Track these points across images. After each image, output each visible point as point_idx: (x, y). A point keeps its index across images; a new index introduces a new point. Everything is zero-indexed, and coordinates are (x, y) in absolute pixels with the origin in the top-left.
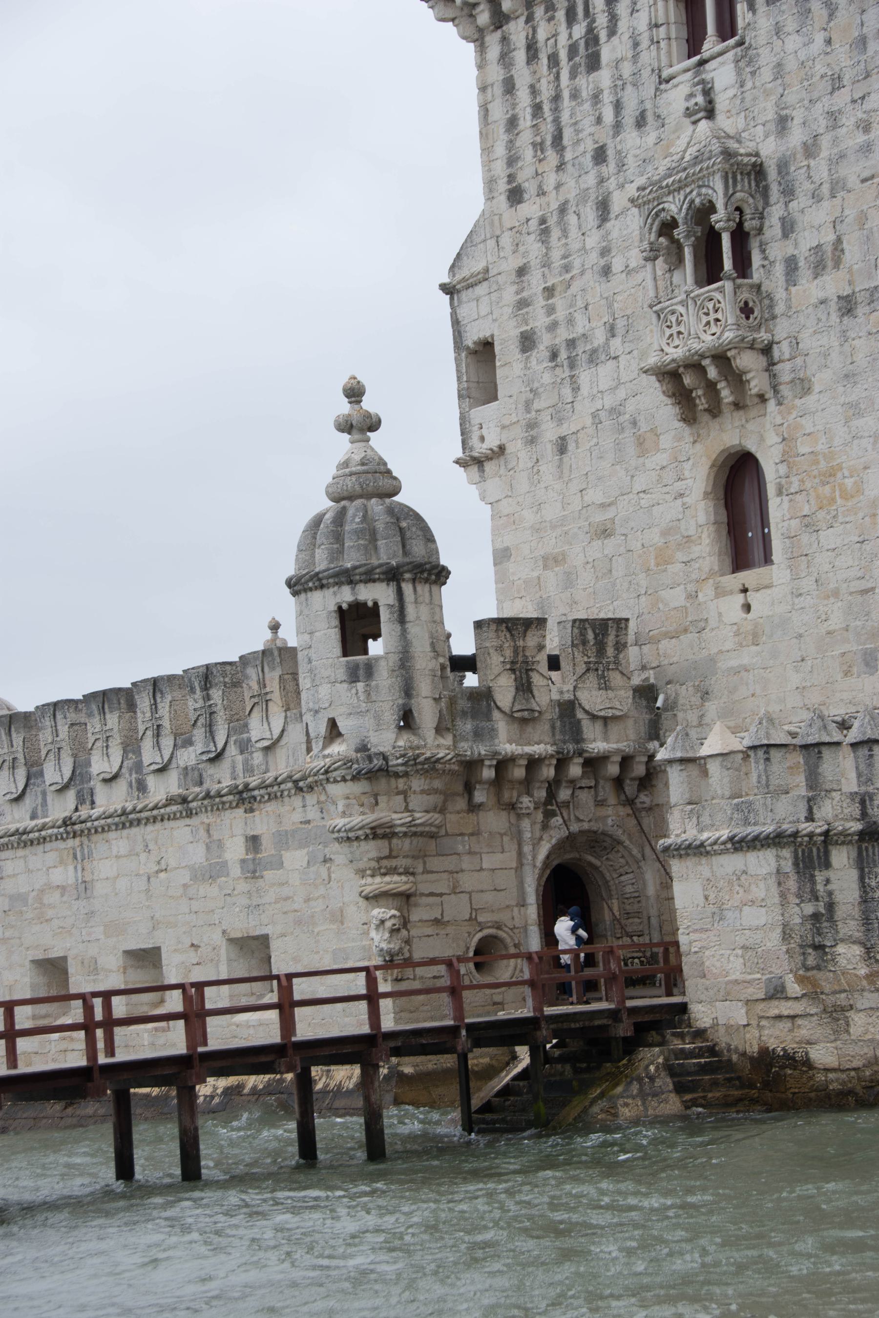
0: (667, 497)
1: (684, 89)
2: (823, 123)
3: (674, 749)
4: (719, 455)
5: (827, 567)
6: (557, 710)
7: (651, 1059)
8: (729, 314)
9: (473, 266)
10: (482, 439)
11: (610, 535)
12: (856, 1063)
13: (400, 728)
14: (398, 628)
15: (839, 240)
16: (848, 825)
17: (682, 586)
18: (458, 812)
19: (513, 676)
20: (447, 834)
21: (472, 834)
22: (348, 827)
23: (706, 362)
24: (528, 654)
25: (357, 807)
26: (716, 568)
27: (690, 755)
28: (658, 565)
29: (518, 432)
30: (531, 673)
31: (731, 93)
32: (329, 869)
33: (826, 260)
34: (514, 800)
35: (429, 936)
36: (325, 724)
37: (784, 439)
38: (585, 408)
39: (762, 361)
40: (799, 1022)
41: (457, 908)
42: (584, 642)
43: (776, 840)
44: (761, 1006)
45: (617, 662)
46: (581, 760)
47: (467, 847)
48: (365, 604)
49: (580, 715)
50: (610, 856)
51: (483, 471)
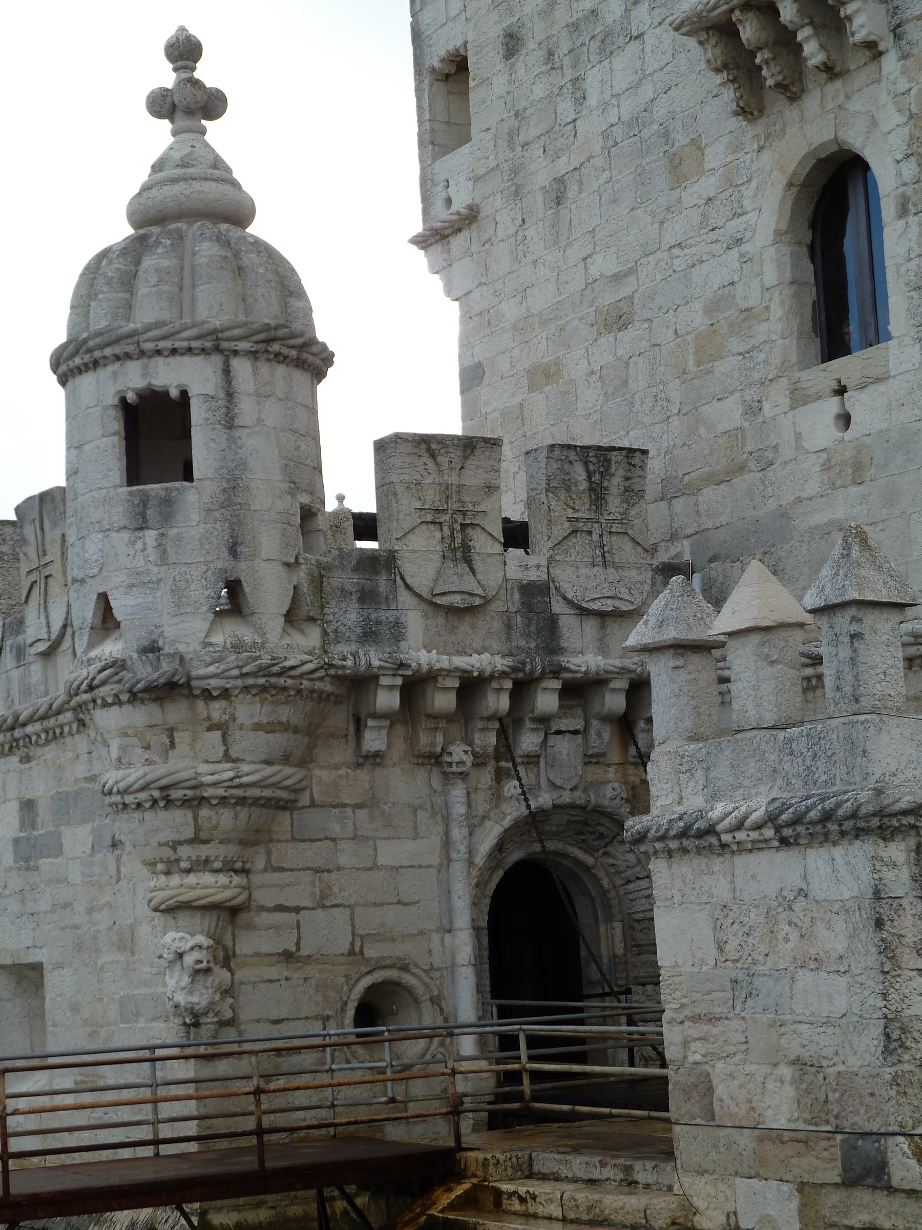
0: (716, 248)
3: (661, 625)
4: (800, 164)
6: (517, 596)
10: (449, 201)
11: (625, 326)
13: (219, 615)
17: (737, 395)
18: (336, 767)
19: (438, 535)
20: (313, 804)
22: (122, 786)
24: (465, 498)
25: (139, 751)
26: (794, 359)
27: (693, 636)
28: (699, 363)
30: (470, 532)
32: (118, 859)
34: (439, 749)
35: (271, 981)
36: (92, 605)
37: (911, 117)
38: (591, 127)
41: (327, 933)
44: (835, 1198)
46: (557, 684)
47: (350, 828)
48: (166, 393)
49: (558, 606)
50: (610, 849)
51: (449, 251)
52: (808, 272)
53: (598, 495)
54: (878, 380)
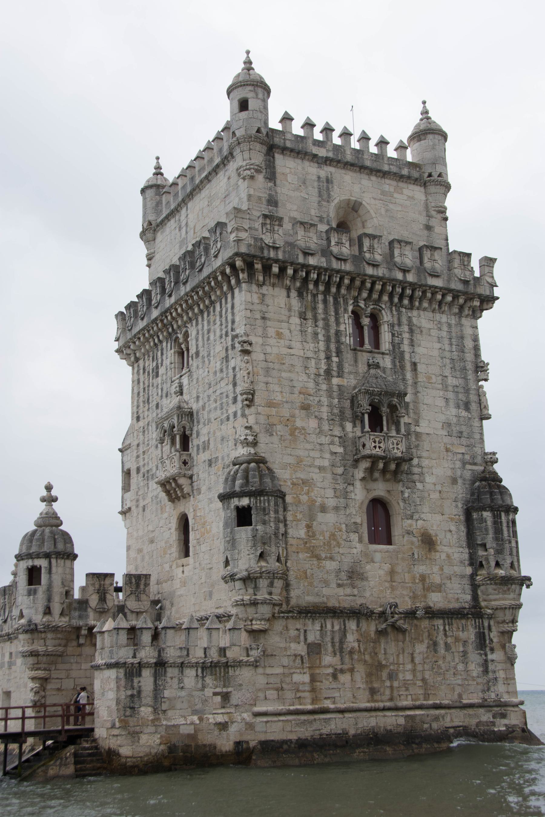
1: (177, 385)
2: (207, 399)
5: (202, 559)
7: (71, 749)
8: (177, 464)
9: (127, 443)
12: (141, 755)
14: (48, 576)
15: (209, 440)
16: (149, 660)
20: (67, 655)
21: (78, 655)
23: (171, 481)
29: (134, 503)
31: (187, 387)
33: (206, 446)
38: (150, 495)
39: (189, 481)
40: (119, 738)
42: (131, 583)
43: (116, 665)
44: (110, 730)
45: (144, 591)
48: (36, 566)
49: (126, 610)
52: (182, 537)
53: (138, 585)
54: (188, 565)
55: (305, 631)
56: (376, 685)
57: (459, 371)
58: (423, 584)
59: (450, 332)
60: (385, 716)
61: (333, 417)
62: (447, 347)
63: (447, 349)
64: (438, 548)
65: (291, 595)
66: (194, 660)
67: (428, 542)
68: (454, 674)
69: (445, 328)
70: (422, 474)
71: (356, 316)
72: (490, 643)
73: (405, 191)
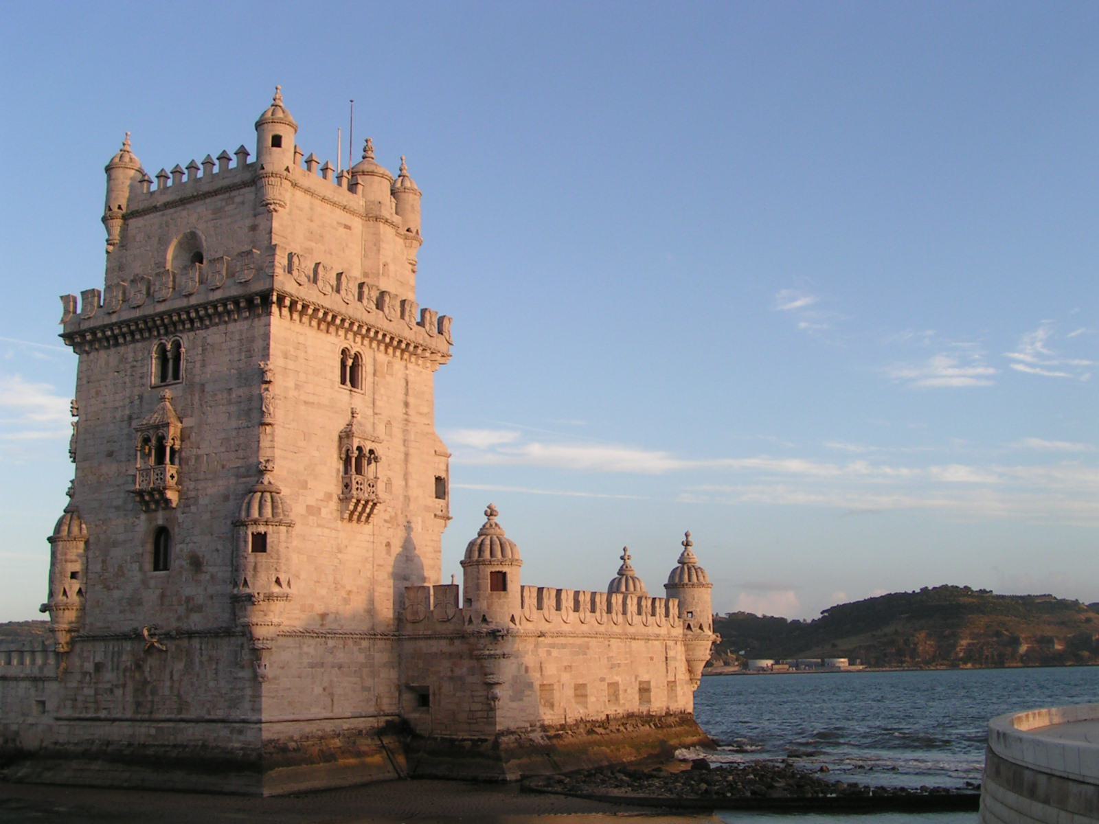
55: (94, 652)
56: (140, 700)
57: (245, 379)
58: (187, 606)
59: (240, 340)
60: (140, 727)
61: (130, 458)
62: (236, 357)
63: (236, 359)
64: (204, 569)
65: (87, 622)
66: (22, 675)
67: (196, 563)
68: (206, 690)
69: (237, 337)
70: (196, 498)
71: (163, 351)
72: (240, 661)
73: (238, 199)
